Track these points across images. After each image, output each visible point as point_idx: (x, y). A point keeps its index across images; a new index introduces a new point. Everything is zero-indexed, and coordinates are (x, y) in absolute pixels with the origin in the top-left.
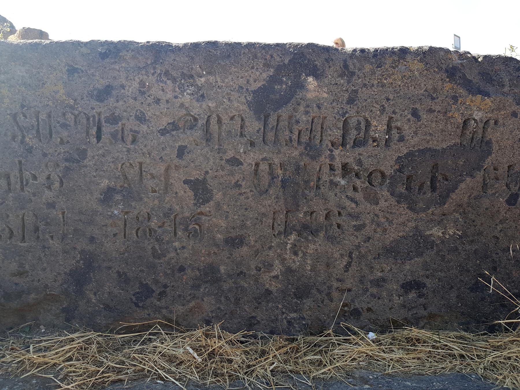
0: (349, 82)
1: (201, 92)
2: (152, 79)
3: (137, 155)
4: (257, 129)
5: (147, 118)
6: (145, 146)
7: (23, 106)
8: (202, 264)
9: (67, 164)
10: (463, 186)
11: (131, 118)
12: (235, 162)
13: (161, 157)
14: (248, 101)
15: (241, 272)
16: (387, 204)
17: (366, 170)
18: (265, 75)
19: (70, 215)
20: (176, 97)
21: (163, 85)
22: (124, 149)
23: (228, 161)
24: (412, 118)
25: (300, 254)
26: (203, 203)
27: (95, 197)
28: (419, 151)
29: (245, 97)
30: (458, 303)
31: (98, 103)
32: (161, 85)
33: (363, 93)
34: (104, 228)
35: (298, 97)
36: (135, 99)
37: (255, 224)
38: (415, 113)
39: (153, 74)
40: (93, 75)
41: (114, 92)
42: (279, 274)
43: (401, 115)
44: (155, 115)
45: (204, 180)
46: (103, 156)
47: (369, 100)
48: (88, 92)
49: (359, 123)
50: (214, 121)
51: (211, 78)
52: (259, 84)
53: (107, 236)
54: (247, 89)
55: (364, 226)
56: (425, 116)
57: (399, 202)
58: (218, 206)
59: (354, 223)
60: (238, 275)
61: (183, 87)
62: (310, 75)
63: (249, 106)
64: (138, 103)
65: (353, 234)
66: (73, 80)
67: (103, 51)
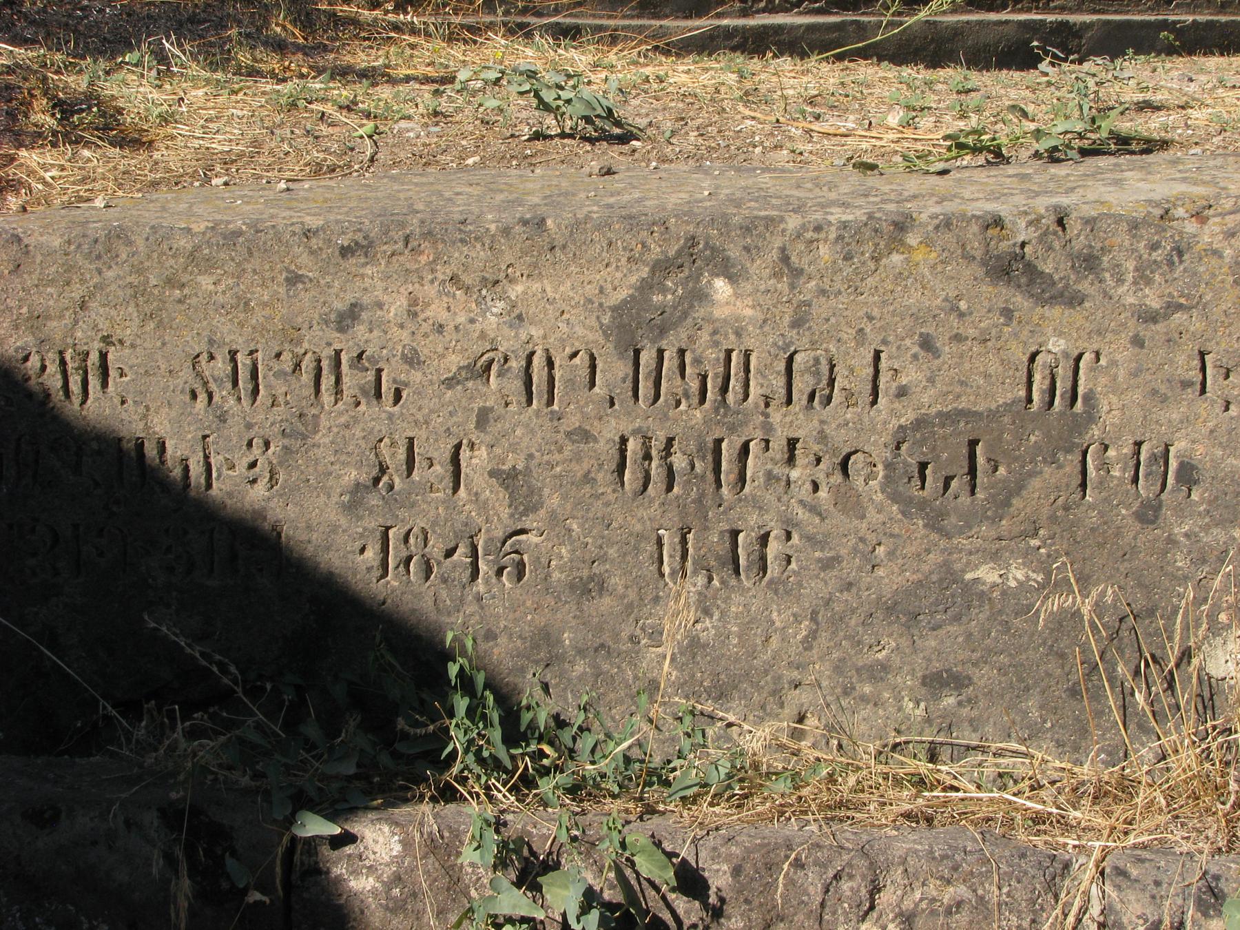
0: (792, 287)
1: (517, 312)
2: (431, 290)
3: (405, 425)
4: (621, 375)
5: (422, 359)
6: (420, 409)
7: (211, 342)
8: (527, 628)
9: (286, 441)
10: (1036, 483)
11: (393, 361)
12: (585, 435)
13: (448, 429)
14: (601, 325)
15: (602, 646)
16: (881, 517)
17: (835, 451)
18: (633, 279)
20: (472, 321)
21: (451, 300)
22: (384, 416)
23: (569, 434)
24: (922, 353)
26: (525, 513)
28: (940, 414)
29: (598, 318)
30: (1045, 721)
31: (338, 335)
32: (445, 299)
33: (820, 308)
34: (350, 556)
35: (696, 315)
36: (402, 326)
37: (625, 554)
38: (927, 344)
39: (432, 282)
40: (329, 287)
41: (364, 316)
43: (899, 348)
44: (435, 352)
45: (528, 471)
46: (347, 427)
47: (833, 320)
48: (320, 316)
49: (817, 361)
50: (538, 361)
51: (536, 286)
52: (623, 294)
54: (601, 305)
55: (837, 559)
56: (947, 348)
58: (554, 518)
59: (817, 554)
62: (717, 275)
63: (604, 333)
64: (405, 335)
65: (817, 577)
66: (295, 296)
67: (346, 244)
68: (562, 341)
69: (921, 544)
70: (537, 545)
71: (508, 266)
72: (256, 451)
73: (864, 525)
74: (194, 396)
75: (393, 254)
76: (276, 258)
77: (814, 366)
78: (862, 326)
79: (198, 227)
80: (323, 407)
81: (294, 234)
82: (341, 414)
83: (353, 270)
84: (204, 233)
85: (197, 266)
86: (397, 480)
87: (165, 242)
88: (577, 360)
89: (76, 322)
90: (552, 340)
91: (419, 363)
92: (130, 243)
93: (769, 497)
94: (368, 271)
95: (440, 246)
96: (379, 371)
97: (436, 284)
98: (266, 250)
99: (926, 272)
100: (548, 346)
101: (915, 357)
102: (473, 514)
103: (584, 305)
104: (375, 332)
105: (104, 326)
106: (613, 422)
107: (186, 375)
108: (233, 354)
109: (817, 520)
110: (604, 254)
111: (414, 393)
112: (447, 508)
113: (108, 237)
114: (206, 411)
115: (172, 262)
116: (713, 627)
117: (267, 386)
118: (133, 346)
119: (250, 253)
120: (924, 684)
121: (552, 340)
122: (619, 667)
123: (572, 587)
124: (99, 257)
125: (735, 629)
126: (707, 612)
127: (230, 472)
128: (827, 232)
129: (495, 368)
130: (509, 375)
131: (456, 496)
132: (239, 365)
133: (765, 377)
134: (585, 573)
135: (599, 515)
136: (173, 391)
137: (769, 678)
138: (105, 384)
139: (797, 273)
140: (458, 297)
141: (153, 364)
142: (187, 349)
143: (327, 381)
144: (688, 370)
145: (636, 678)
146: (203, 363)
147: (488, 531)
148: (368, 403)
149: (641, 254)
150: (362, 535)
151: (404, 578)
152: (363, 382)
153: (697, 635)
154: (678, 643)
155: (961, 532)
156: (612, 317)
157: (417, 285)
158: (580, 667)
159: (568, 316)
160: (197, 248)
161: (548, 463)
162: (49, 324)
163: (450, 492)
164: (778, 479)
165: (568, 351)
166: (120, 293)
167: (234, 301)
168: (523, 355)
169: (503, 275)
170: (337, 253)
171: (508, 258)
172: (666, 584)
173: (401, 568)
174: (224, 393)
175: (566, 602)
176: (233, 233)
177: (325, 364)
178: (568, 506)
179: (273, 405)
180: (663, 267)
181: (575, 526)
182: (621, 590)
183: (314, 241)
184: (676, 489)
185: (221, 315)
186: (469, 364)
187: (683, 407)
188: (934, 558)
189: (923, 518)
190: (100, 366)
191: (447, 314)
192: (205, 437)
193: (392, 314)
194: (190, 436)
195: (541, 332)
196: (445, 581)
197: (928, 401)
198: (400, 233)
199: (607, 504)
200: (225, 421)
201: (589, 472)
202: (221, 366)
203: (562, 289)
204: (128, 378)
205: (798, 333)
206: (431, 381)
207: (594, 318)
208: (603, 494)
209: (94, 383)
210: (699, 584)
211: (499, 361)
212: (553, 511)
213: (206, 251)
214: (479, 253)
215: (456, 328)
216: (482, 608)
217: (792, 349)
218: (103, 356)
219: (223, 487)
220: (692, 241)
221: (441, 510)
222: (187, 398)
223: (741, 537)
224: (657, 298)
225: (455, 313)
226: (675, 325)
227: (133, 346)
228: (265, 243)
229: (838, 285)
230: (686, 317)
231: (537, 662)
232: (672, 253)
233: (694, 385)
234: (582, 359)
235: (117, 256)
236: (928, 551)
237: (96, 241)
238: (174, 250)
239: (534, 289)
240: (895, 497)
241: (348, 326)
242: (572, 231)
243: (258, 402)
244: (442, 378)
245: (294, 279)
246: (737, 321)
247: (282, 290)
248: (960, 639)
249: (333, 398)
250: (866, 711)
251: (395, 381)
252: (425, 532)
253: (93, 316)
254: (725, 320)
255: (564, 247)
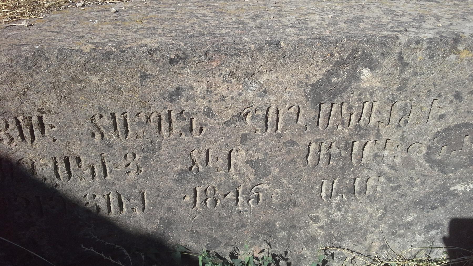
0: (401, 71)
2: (219, 80)
4: (313, 116)
5: (214, 113)
6: (213, 136)
7: (100, 109)
9: (145, 154)
11: (199, 114)
12: (293, 143)
13: (227, 144)
15: (293, 226)
16: (421, 169)
18: (324, 71)
19: (150, 193)
20: (240, 94)
21: (229, 84)
22: (194, 140)
23: (285, 143)
24: (455, 100)
25: (343, 210)
27: (171, 178)
28: (456, 126)
29: (304, 90)
31: (170, 104)
32: (226, 84)
33: (413, 81)
34: (179, 200)
35: (352, 87)
36: (204, 98)
37: (307, 191)
38: (458, 96)
39: (220, 75)
40: (164, 80)
42: (324, 225)
46: (176, 146)
47: (417, 87)
48: (160, 95)
49: (406, 105)
51: (274, 76)
52: (318, 77)
53: (181, 206)
54: (306, 84)
55: (399, 186)
57: (432, 167)
59: (391, 185)
60: (290, 227)
61: (246, 85)
62: (366, 67)
64: (205, 103)
65: (389, 194)
66: (146, 85)
67: (172, 57)
68: (286, 102)
69: (435, 178)
70: (267, 189)
71: (260, 67)
72: (129, 159)
73: (413, 173)
74: (93, 135)
75: (198, 62)
76: (133, 66)
77: (404, 107)
78: (431, 89)
79: (87, 48)
80: (163, 138)
81: (143, 53)
82: (172, 140)
83: (177, 71)
84: (90, 53)
85: (88, 71)
86: (201, 167)
87: (68, 59)
88: (291, 110)
89: (22, 103)
90: (280, 101)
91: (212, 115)
92: (47, 59)
93: (374, 164)
94: (186, 71)
95: (224, 57)
96: (191, 120)
97: (222, 76)
98: (128, 62)
99: (465, 63)
100: (278, 104)
101: (451, 102)
102: (238, 179)
103: (298, 84)
104: (190, 101)
105: (39, 104)
106: (307, 137)
107: (87, 126)
108: (113, 115)
109: (393, 172)
110: (311, 59)
111: (210, 129)
112: (225, 178)
113: (34, 56)
114: (101, 143)
115: (73, 69)
116: (341, 215)
117: (133, 130)
118: (56, 113)
119: (119, 64)
120: (425, 229)
121: (280, 101)
122: (299, 232)
123: (281, 205)
124: (30, 68)
125: (350, 215)
126: (339, 210)
127: (116, 169)
128: (422, 45)
129: (249, 116)
130: (258, 118)
131: (229, 172)
132: (117, 120)
133: (380, 113)
134: (288, 199)
135: (296, 176)
136: (82, 134)
137: (362, 231)
138: (43, 132)
139: (405, 65)
140: (233, 82)
141: (69, 121)
142: (87, 113)
143: (164, 125)
144: (344, 112)
145: (306, 236)
146: (97, 120)
147: (244, 186)
148: (186, 135)
149: (330, 59)
150: (184, 192)
151: (205, 207)
152: (183, 125)
153: (334, 218)
154: (326, 222)
155: (452, 172)
156: (312, 90)
157: (211, 77)
158: (283, 234)
159: (289, 90)
160: (87, 62)
161: (274, 156)
162: (6, 104)
163: (226, 171)
164: (379, 156)
165: (288, 106)
166: (45, 86)
167: (112, 88)
168: (265, 109)
169: (257, 71)
170: (168, 62)
171: (260, 63)
172: (323, 201)
173: (203, 203)
174: (110, 134)
175: (278, 211)
176: (108, 52)
177: (163, 117)
178: (283, 174)
179: (137, 138)
180: (338, 64)
181: (285, 181)
182: (303, 204)
183: (154, 56)
184: (331, 163)
185: (105, 96)
186: (238, 114)
187: (340, 128)
188: (439, 183)
189: (438, 168)
190: (39, 124)
191: (227, 91)
192: (101, 154)
193: (198, 92)
194: (93, 155)
195: (275, 98)
196: (223, 206)
197: (452, 121)
198: (202, 51)
199: (300, 172)
200: (112, 147)
201: (294, 159)
202: (107, 120)
203: (287, 77)
204: (55, 129)
205: (400, 93)
206: (218, 123)
207: (302, 91)
208: (299, 167)
209: (37, 132)
210: (338, 200)
211: (253, 112)
212: (276, 176)
213: (93, 63)
214: (245, 61)
215: (232, 97)
216: (240, 216)
217: (396, 100)
218: (40, 119)
219: (113, 176)
220: (355, 50)
221: (222, 178)
222: (90, 137)
223: (358, 180)
224: (334, 80)
225: (232, 91)
226: (341, 92)
227: (56, 113)
228: (127, 58)
229: (422, 70)
230: (347, 88)
231: (264, 234)
232: (345, 57)
233: (347, 119)
234: (294, 109)
235: (41, 66)
236: (438, 180)
237: (27, 59)
238: (74, 63)
239: (273, 77)
240: (428, 162)
241: (175, 99)
242: (295, 48)
243: (128, 137)
244: (224, 122)
245: (144, 77)
246: (371, 89)
247: (138, 82)
248: (443, 211)
249: (168, 133)
250: (400, 240)
251: (200, 124)
252: (214, 188)
253: (31, 99)
254: (366, 89)
255: (290, 56)
